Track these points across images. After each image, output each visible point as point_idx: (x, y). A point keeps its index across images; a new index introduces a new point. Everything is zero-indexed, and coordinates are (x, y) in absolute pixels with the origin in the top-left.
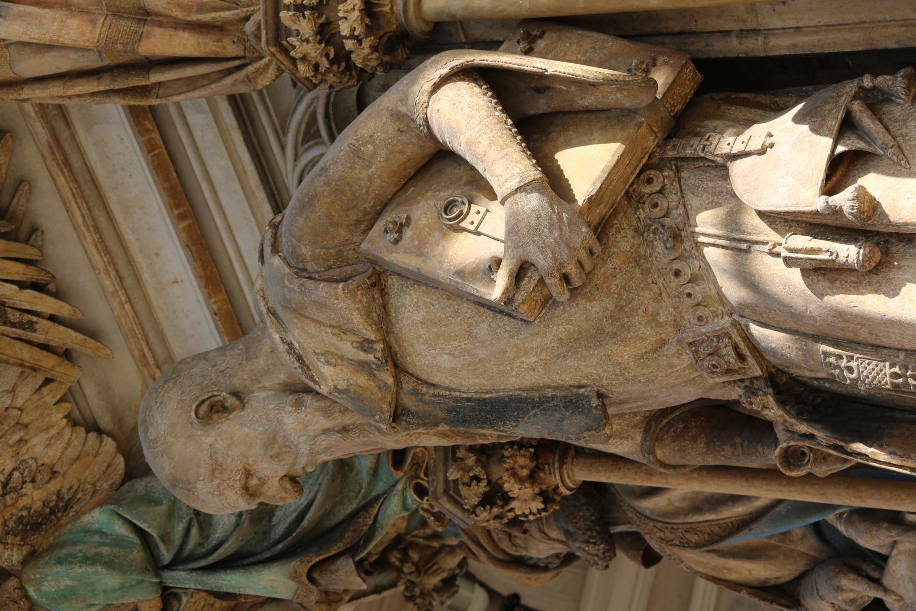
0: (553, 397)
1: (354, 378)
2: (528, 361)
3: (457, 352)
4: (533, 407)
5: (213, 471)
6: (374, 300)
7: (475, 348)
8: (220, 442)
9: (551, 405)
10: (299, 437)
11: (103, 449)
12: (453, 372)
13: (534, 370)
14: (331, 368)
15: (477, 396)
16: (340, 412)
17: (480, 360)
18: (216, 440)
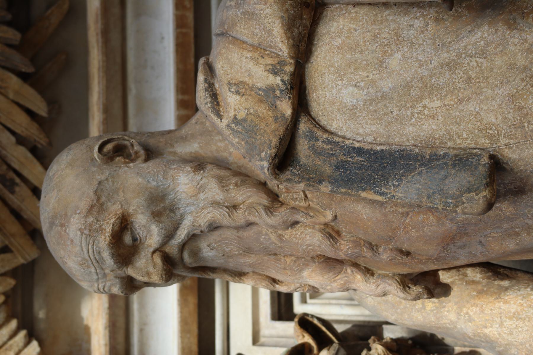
0: (445, 155)
1: (256, 107)
2: (431, 105)
3: (362, 84)
4: (420, 166)
5: (92, 207)
6: (301, 18)
7: (381, 79)
8: (111, 183)
9: (440, 162)
10: (188, 205)
11: (26, 350)
12: (353, 111)
13: (434, 118)
14: (238, 97)
15: (368, 147)
16: (236, 185)
17: (383, 96)
18: (107, 179)
